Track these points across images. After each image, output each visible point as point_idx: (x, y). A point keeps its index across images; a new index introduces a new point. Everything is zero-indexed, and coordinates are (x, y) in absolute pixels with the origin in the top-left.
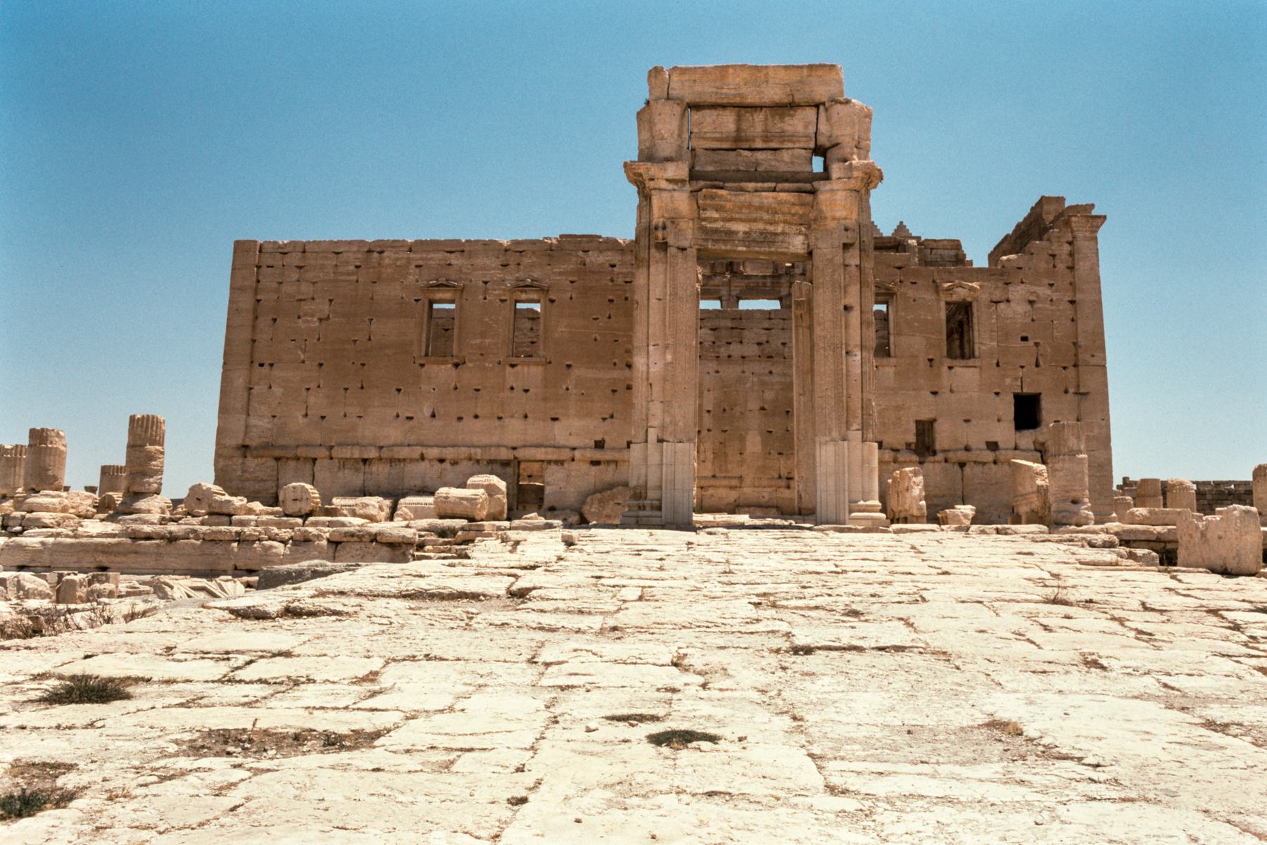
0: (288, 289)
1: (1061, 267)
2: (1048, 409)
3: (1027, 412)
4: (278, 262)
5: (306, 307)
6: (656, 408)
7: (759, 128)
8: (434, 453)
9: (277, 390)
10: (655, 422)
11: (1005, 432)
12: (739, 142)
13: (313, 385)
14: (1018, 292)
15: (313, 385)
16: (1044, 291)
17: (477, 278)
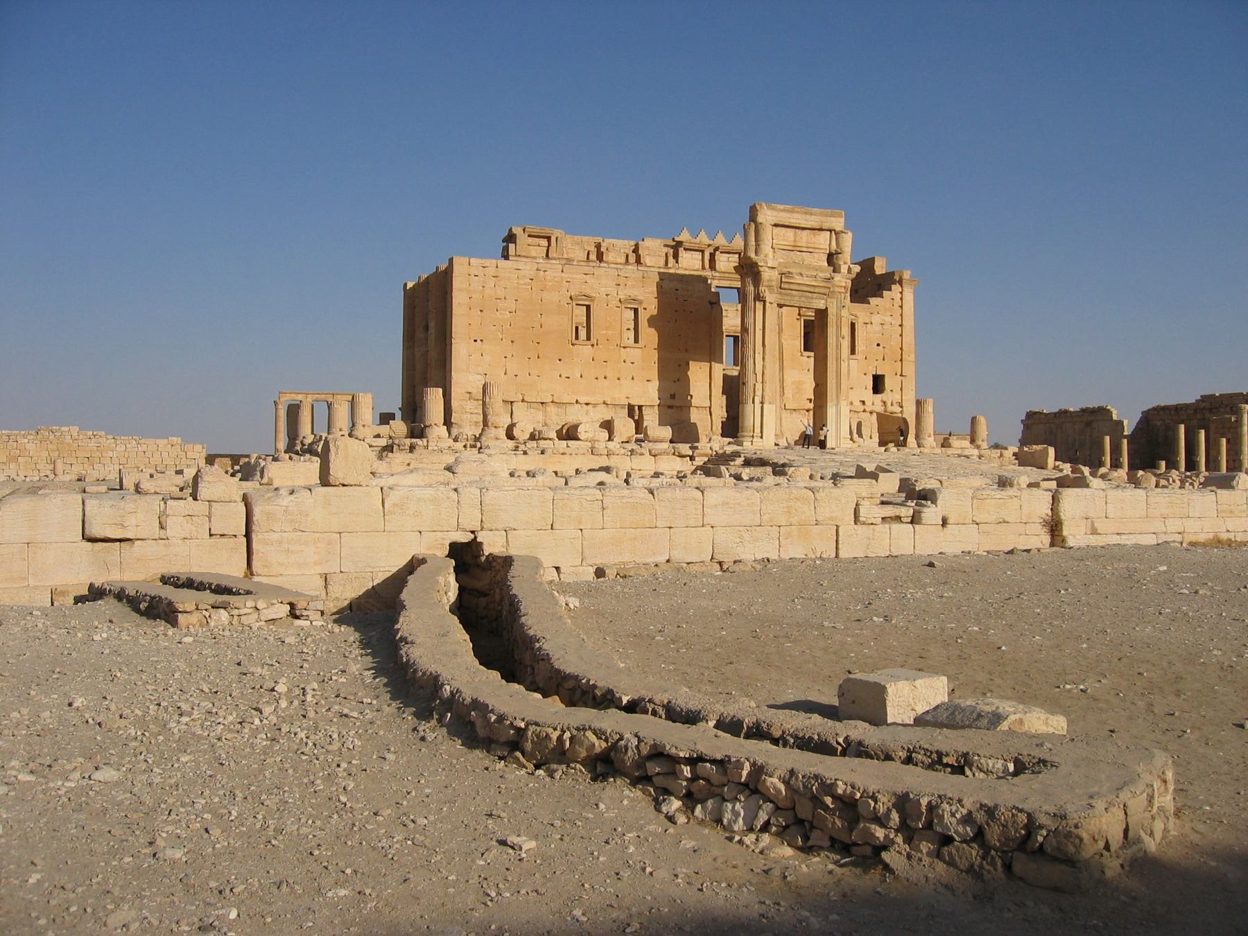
0: (488, 291)
1: (896, 306)
2: (888, 383)
3: (878, 384)
4: (480, 272)
5: (501, 304)
6: (759, 386)
7: (804, 240)
8: (583, 400)
9: (487, 358)
10: (759, 393)
11: (868, 395)
12: (795, 248)
13: (509, 356)
14: (876, 319)
15: (509, 356)
16: (888, 319)
17: (603, 291)
